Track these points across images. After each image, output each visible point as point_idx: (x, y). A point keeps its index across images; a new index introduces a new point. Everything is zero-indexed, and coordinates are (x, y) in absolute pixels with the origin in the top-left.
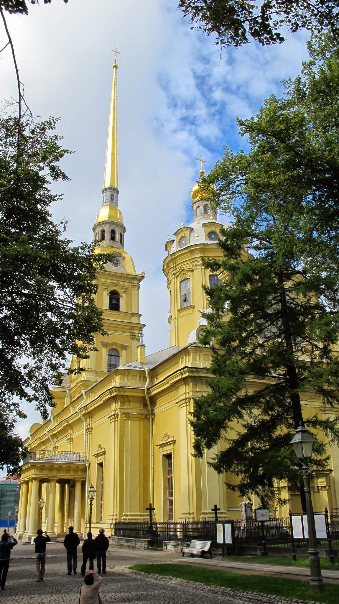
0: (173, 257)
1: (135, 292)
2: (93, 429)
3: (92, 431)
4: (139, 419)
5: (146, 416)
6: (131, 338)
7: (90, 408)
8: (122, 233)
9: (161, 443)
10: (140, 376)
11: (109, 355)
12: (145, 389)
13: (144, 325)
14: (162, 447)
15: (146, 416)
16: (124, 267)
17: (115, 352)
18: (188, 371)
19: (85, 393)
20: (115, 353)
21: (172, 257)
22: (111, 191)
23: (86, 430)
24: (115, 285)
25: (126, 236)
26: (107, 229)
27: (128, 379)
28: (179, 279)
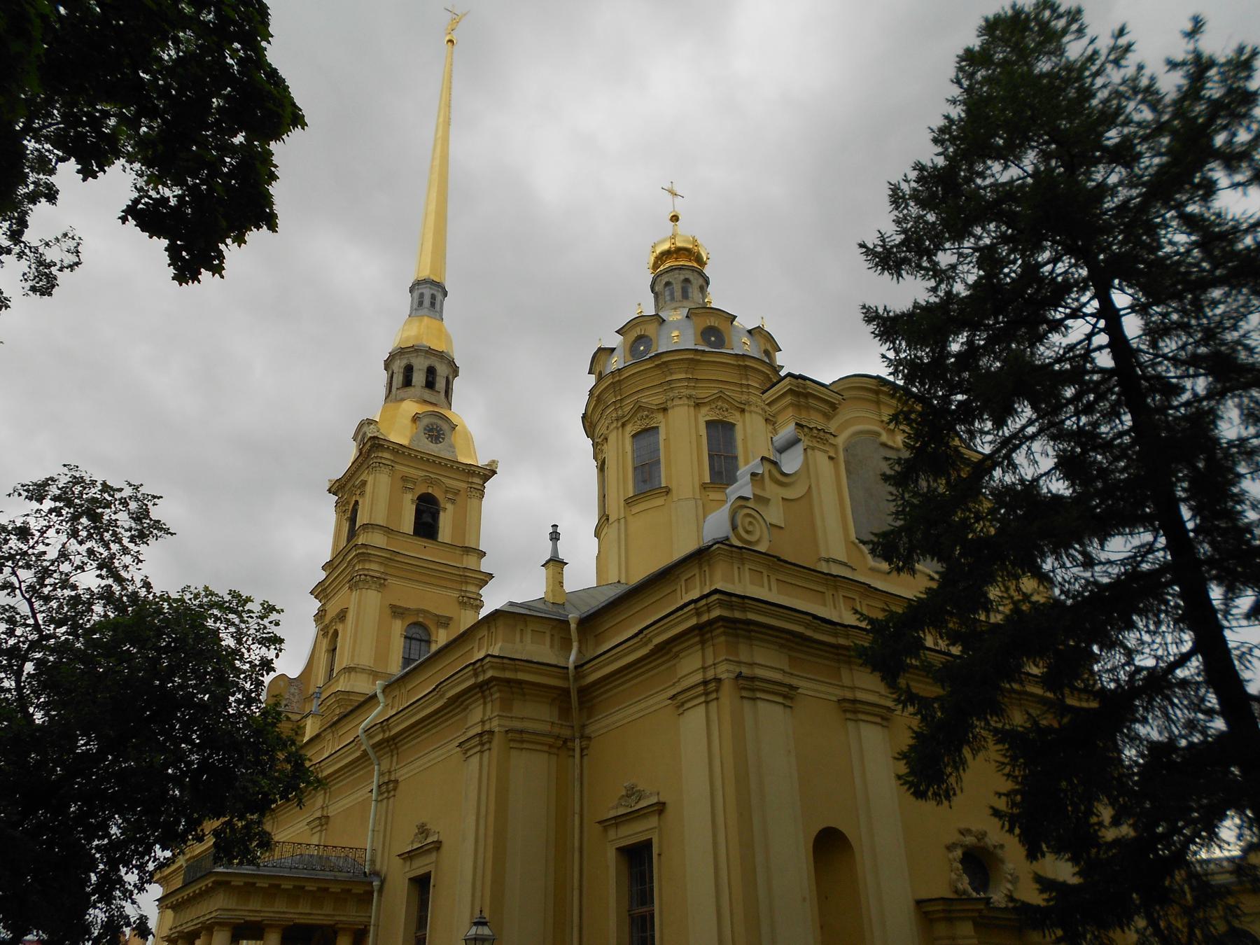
0: (617, 378)
1: (475, 501)
2: (401, 786)
3: (395, 789)
4: (546, 748)
5: (565, 741)
6: (460, 603)
7: (398, 724)
8: (451, 377)
9: (612, 814)
10: (552, 635)
11: (406, 637)
13: (491, 576)
14: (617, 825)
15: (565, 741)
16: (452, 446)
17: (420, 632)
18: (721, 603)
19: (383, 691)
20: (419, 632)
22: (430, 288)
23: (379, 786)
24: (430, 482)
25: (457, 384)
26: (420, 364)
27: (521, 641)
28: (630, 429)
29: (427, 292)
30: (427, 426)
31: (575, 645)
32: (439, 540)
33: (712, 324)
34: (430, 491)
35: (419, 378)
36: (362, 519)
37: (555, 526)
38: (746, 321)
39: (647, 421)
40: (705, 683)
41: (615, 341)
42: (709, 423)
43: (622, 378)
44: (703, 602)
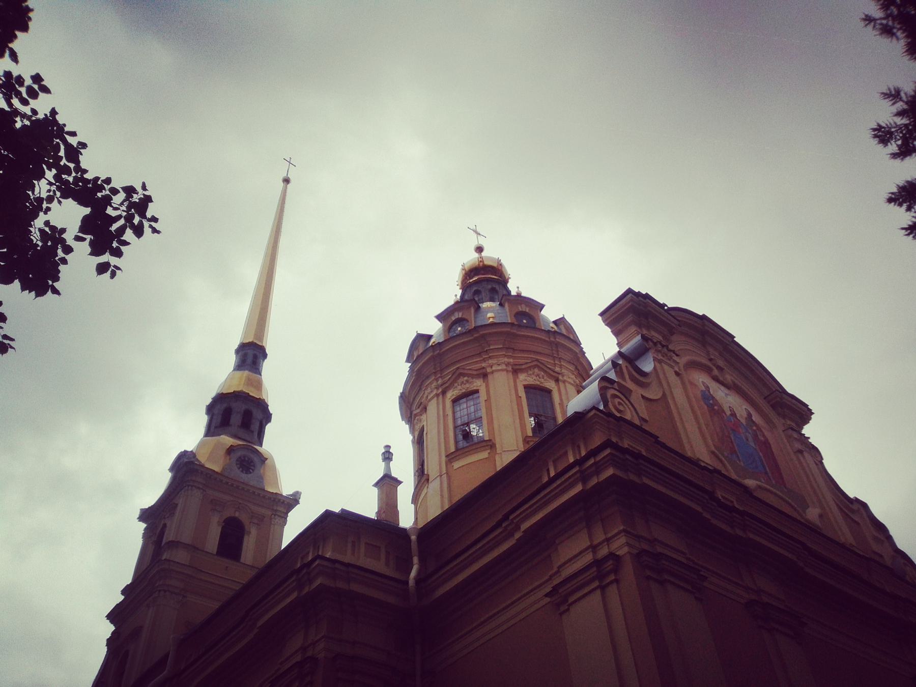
8: (264, 423)
12: (411, 582)
16: (261, 478)
21: (434, 352)
29: (251, 353)
30: (240, 458)
31: (416, 560)
32: (242, 560)
33: (524, 310)
34: (237, 515)
35: (236, 419)
36: (169, 536)
37: (388, 447)
38: (550, 314)
39: (467, 385)
40: (597, 563)
41: (434, 328)
42: (527, 387)
43: (442, 351)
44: (592, 461)
